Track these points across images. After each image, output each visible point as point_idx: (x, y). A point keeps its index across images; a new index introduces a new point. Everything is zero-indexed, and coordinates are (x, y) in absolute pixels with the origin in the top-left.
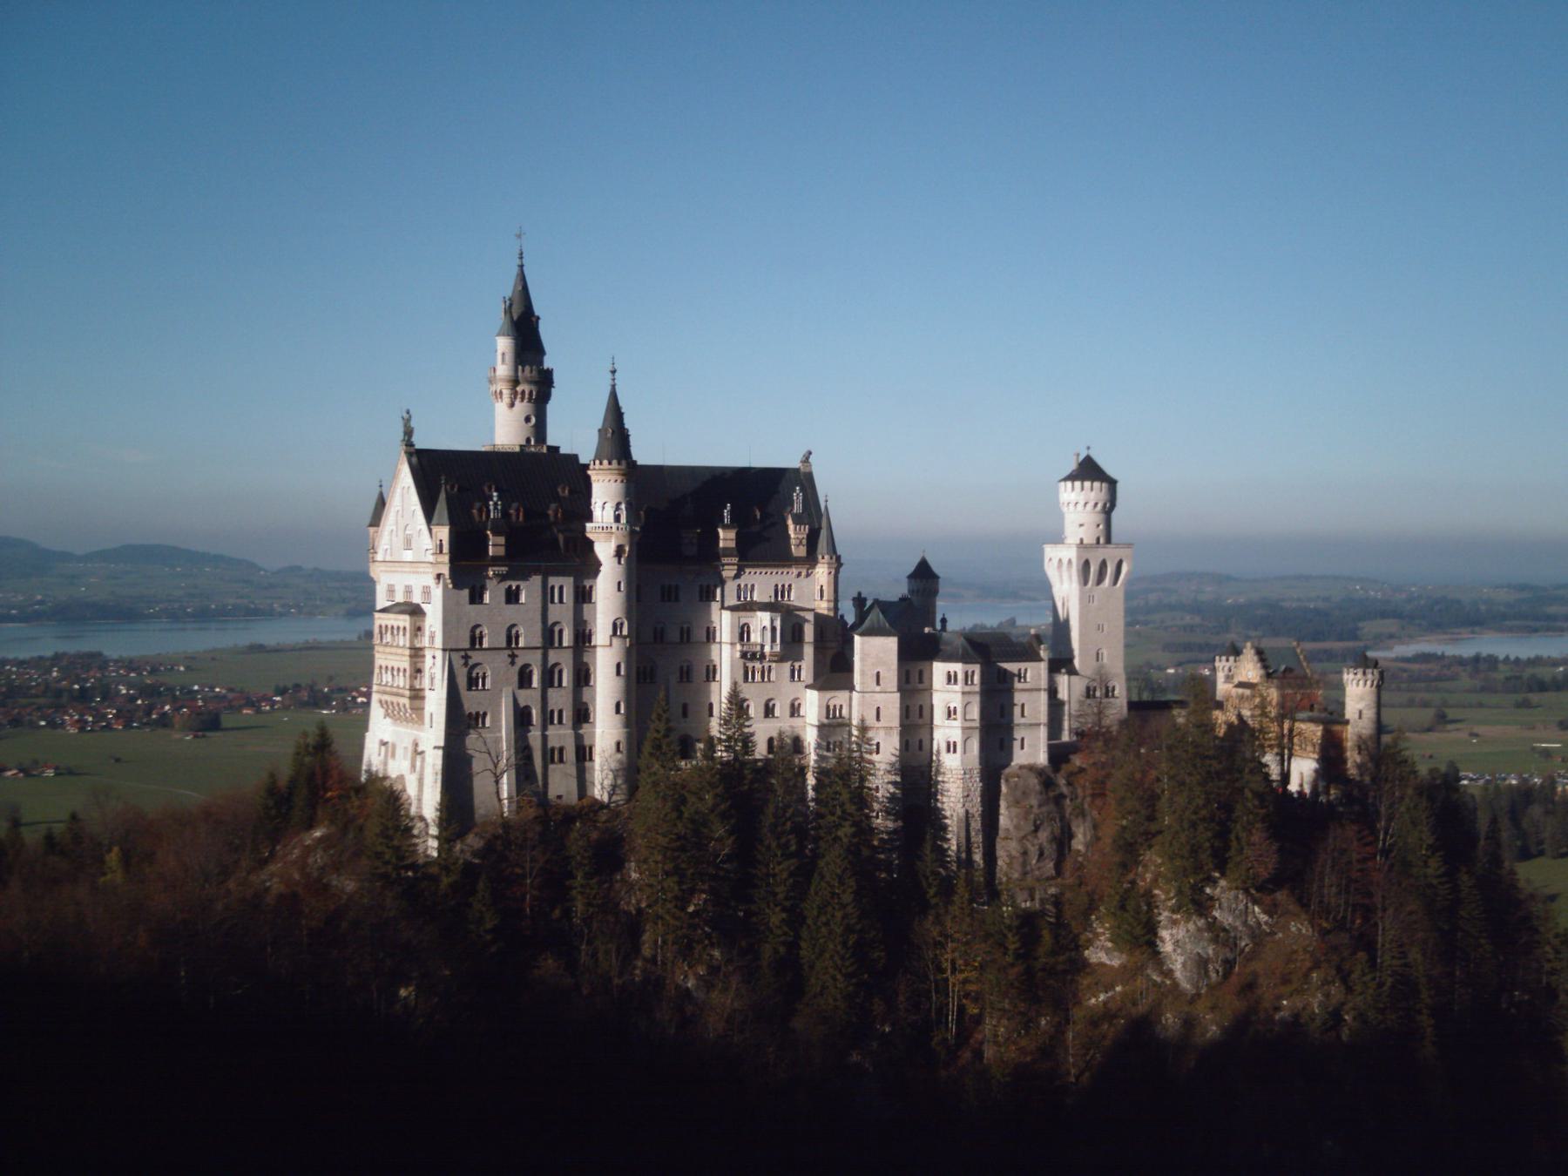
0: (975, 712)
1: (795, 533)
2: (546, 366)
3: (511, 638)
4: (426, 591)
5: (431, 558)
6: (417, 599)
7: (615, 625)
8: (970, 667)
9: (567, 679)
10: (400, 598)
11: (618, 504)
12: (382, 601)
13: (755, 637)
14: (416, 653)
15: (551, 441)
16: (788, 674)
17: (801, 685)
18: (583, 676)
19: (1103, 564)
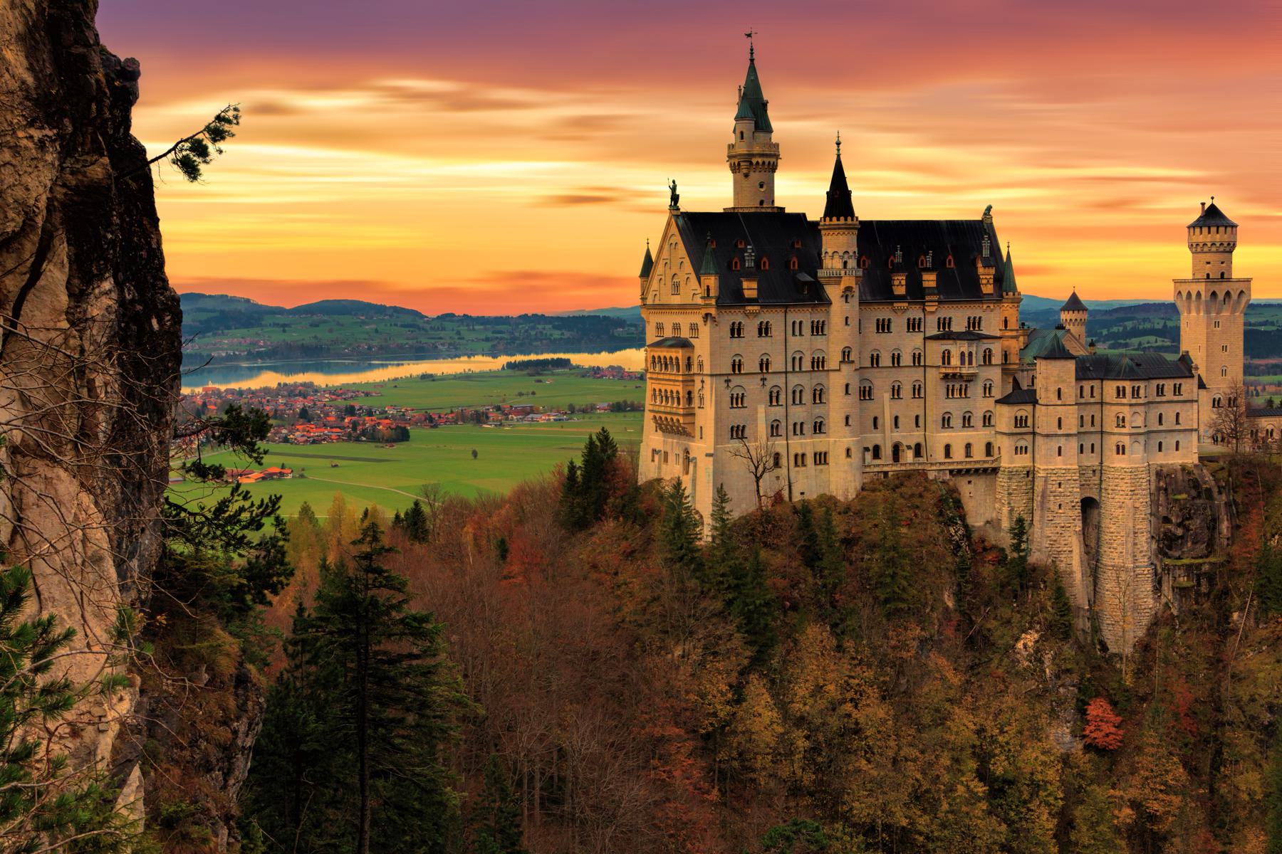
0: (1139, 421)
1: (986, 275)
2: (774, 141)
3: (764, 365)
4: (694, 328)
5: (700, 301)
6: (685, 333)
7: (844, 352)
8: (1136, 384)
9: (807, 397)
10: (668, 333)
11: (846, 252)
12: (651, 337)
13: (955, 361)
14: (689, 380)
15: (776, 204)
16: (981, 390)
17: (992, 400)
18: (819, 395)
19: (1228, 294)
